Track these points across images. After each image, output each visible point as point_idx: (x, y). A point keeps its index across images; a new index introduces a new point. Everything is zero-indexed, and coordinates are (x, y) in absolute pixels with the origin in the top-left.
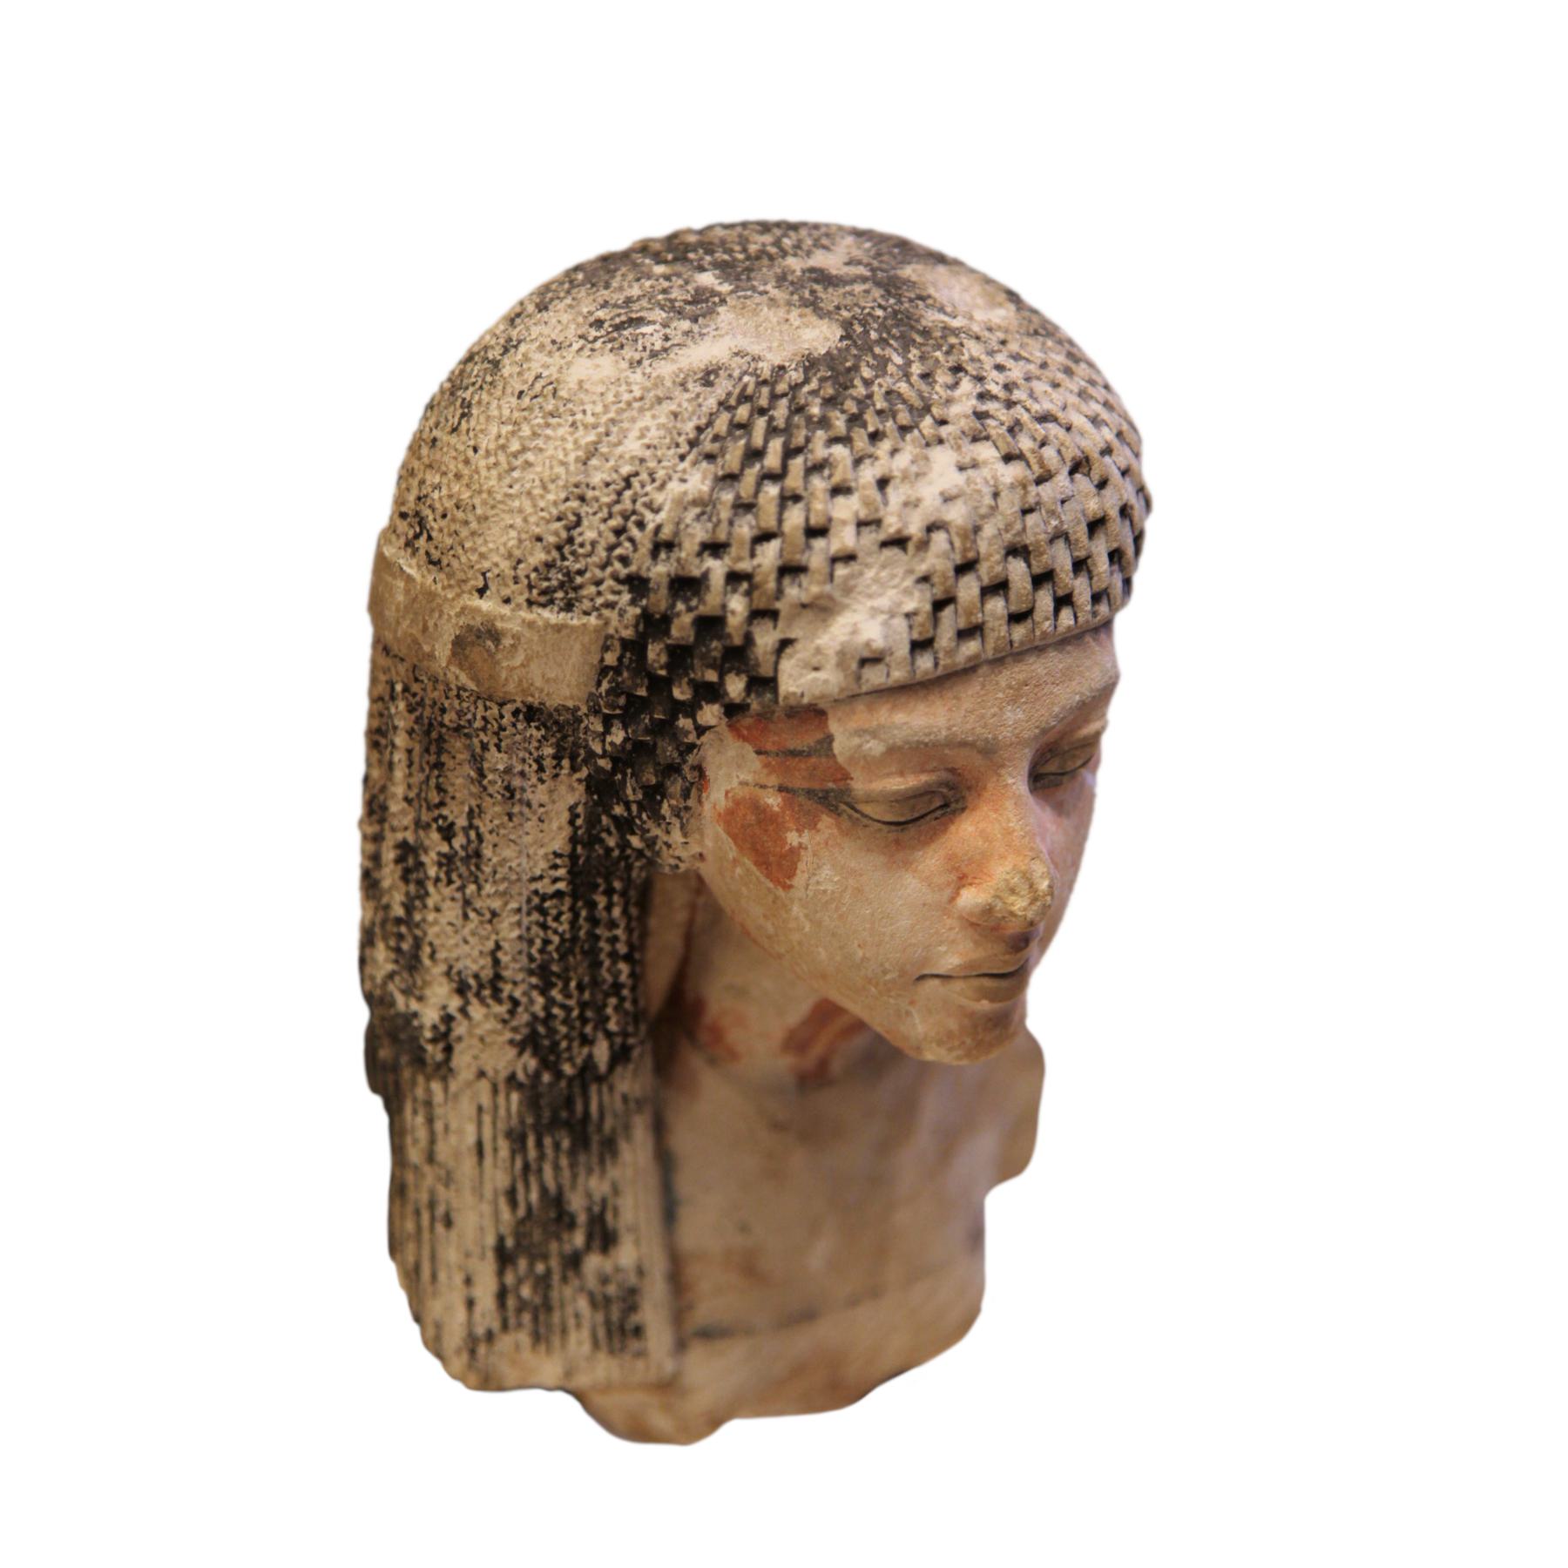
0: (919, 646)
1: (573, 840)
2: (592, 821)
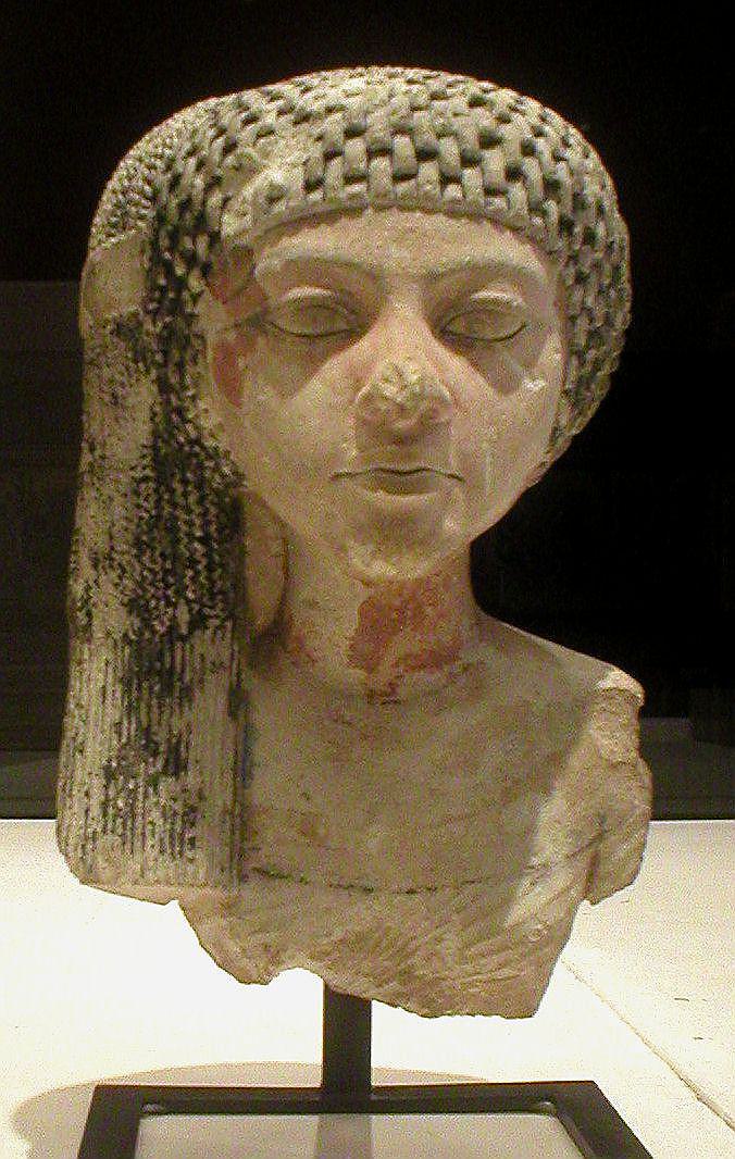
0: (310, 186)
1: (155, 434)
2: (169, 421)
